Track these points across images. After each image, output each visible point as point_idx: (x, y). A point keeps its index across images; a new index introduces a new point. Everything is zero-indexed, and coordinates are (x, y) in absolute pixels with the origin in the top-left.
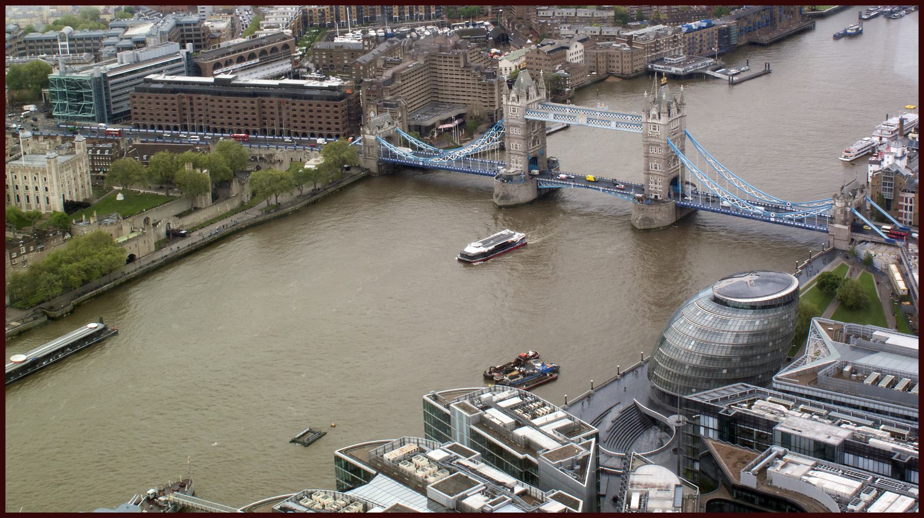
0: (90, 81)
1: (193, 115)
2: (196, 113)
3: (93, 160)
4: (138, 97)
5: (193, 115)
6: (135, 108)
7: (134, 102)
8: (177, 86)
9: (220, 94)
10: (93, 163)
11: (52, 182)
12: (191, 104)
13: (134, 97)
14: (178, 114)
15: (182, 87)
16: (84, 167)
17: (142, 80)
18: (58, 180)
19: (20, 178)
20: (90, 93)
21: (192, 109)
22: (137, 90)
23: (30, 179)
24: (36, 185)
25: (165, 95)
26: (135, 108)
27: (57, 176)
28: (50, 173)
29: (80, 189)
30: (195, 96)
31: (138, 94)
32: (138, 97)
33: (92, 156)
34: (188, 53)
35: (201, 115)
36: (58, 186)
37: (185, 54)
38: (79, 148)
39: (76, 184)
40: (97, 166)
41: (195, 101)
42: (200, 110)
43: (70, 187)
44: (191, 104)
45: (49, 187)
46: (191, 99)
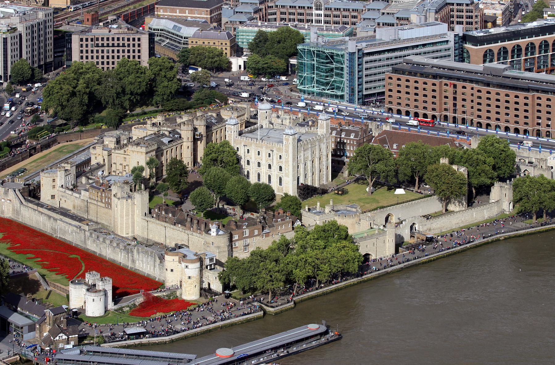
5: (455, 105)
6: (390, 90)
7: (390, 84)
8: (441, 71)
9: (488, 85)
11: (287, 162)
13: (390, 78)
14: (438, 103)
17: (401, 60)
21: (455, 99)
22: (395, 71)
23: (264, 154)
26: (390, 90)
28: (287, 152)
30: (460, 84)
31: (395, 76)
34: (455, 36)
37: (453, 36)
38: (322, 127)
41: (459, 90)
46: (455, 86)
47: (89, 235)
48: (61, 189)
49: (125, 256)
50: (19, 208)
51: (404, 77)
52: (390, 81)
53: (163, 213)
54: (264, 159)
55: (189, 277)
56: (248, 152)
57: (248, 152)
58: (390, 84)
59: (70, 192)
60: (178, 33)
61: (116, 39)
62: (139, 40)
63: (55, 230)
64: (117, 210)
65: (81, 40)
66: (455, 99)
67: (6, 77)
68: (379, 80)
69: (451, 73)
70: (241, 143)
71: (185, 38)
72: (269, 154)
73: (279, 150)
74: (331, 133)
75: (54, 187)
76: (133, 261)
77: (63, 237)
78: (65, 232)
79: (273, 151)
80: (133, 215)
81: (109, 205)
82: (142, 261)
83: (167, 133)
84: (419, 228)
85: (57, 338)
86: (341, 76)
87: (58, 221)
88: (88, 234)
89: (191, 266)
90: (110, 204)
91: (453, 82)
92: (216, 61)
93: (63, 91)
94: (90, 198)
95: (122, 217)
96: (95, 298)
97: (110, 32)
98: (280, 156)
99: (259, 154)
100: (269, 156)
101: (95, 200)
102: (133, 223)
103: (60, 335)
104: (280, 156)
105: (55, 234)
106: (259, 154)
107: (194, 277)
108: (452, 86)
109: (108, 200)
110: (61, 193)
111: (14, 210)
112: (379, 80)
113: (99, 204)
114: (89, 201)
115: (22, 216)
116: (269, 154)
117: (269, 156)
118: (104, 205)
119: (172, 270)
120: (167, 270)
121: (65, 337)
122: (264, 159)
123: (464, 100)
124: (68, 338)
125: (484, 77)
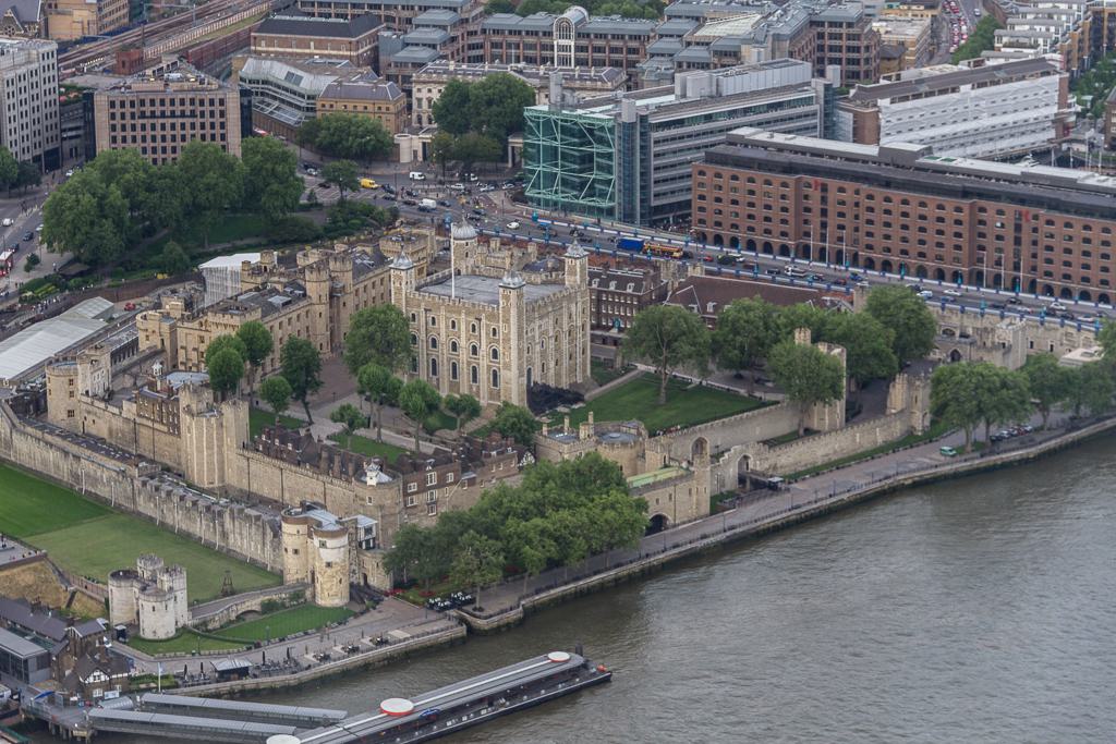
0: (611, 130)
1: (824, 225)
2: (833, 220)
3: (599, 302)
4: (710, 174)
5: (824, 225)
6: (702, 197)
7: (701, 185)
8: (798, 159)
9: (888, 184)
11: (507, 340)
12: (824, 200)
13: (702, 173)
14: (792, 221)
15: (807, 160)
16: (579, 313)
17: (722, 137)
19: (442, 325)
20: (609, 156)
21: (824, 213)
22: (712, 159)
24: (475, 342)
25: (768, 175)
26: (702, 197)
27: (520, 328)
28: (507, 321)
29: (565, 362)
30: (833, 184)
31: (711, 169)
32: (710, 174)
33: (600, 292)
34: (827, 87)
35: (841, 227)
36: (520, 351)
37: (821, 89)
39: (558, 349)
40: (607, 315)
41: (833, 195)
42: (841, 215)
43: (543, 354)
44: (824, 200)
45: (500, 350)
46: (824, 188)
48: (85, 399)
49: (208, 526)
51: (727, 171)
52: (701, 178)
53: (277, 442)
54: (463, 335)
55: (329, 565)
56: (434, 323)
57: (434, 323)
58: (701, 185)
59: (102, 405)
60: (295, 88)
61: (177, 102)
62: (222, 102)
63: (77, 477)
65: (112, 104)
66: (824, 213)
68: (682, 177)
69: (817, 161)
71: (309, 98)
72: (474, 326)
73: (493, 317)
74: (590, 284)
75: (72, 394)
76: (224, 535)
78: (95, 481)
80: (220, 447)
81: (175, 429)
82: (241, 534)
83: (279, 287)
84: (755, 465)
85: (91, 680)
86: (609, 170)
87: (82, 460)
88: (138, 483)
89: (330, 543)
91: (820, 179)
92: (370, 140)
93: (80, 207)
95: (200, 451)
96: (157, 605)
98: (494, 329)
99: (454, 327)
100: (474, 330)
101: (148, 419)
102: (221, 463)
103: (95, 674)
104: (494, 329)
105: (78, 484)
106: (454, 327)
108: (819, 188)
110: (84, 407)
112: (682, 177)
113: (157, 426)
114: (138, 420)
115: (16, 452)
116: (474, 326)
117: (474, 330)
118: (165, 429)
119: (296, 552)
120: (286, 550)
121: (103, 678)
122: (463, 335)
123: (841, 215)
124: (111, 679)
125: (879, 170)
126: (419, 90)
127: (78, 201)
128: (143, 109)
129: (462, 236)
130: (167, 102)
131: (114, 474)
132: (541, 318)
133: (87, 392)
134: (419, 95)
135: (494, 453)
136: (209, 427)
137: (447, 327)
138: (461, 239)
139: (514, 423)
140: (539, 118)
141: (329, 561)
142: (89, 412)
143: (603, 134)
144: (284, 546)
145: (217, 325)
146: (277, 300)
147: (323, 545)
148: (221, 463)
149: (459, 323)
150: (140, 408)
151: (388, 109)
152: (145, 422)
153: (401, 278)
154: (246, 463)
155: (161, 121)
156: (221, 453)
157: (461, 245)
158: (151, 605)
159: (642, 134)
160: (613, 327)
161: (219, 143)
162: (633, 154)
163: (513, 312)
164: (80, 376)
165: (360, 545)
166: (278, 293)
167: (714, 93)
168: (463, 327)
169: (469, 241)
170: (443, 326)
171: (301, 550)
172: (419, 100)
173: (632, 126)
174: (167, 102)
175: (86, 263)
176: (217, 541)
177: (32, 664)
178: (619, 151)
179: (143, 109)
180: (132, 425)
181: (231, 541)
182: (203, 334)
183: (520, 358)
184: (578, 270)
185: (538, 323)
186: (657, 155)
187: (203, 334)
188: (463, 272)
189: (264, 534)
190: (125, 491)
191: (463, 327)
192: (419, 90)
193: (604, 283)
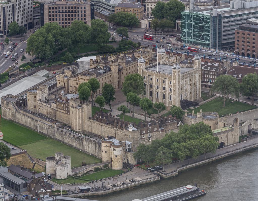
0: (209, 19)
3: (204, 74)
4: (241, 33)
6: (238, 41)
7: (238, 37)
10: (204, 76)
11: (175, 85)
13: (238, 33)
16: (198, 77)
17: (245, 21)
18: (179, 84)
19: (154, 80)
20: (209, 27)
22: (241, 28)
24: (164, 86)
26: (238, 41)
27: (179, 82)
28: (175, 79)
29: (193, 92)
31: (241, 31)
32: (241, 33)
33: (205, 71)
36: (179, 89)
38: (196, 64)
39: (191, 89)
40: (207, 78)
43: (186, 90)
45: (172, 89)
47: (56, 130)
48: (39, 102)
50: (15, 113)
51: (246, 32)
52: (238, 35)
54: (161, 84)
55: (116, 156)
56: (151, 80)
57: (151, 80)
58: (238, 37)
59: (45, 104)
60: (108, 4)
61: (70, 8)
62: (85, 8)
64: (73, 115)
65: (50, 8)
67: (5, 32)
68: (232, 34)
70: (147, 74)
71: (112, 7)
72: (164, 81)
73: (170, 78)
74: (202, 68)
76: (83, 146)
77: (41, 131)
78: (42, 128)
79: (166, 79)
80: (82, 118)
81: (68, 112)
82: (88, 146)
83: (102, 67)
84: (253, 127)
85: (40, 191)
86: (208, 31)
87: (38, 122)
88: (56, 129)
89: (117, 149)
90: (69, 112)
92: (132, 21)
93: (39, 41)
94: (57, 108)
97: (67, 2)
98: (170, 82)
100: (164, 82)
101: (59, 109)
102: (83, 123)
103: (41, 190)
104: (170, 82)
105: (37, 129)
107: (119, 156)
109: (67, 109)
110: (39, 105)
111: (12, 114)
112: (232, 34)
113: (62, 111)
114: (56, 109)
116: (164, 81)
117: (164, 82)
118: (65, 112)
119: (106, 152)
120: (103, 151)
122: (161, 84)
126: (148, 5)
127: (38, 39)
128: (59, 10)
129: (161, 52)
130: (67, 8)
131: (48, 126)
132: (186, 78)
133: (40, 100)
134: (148, 7)
135: (170, 121)
136: (79, 111)
137: (155, 81)
138: (160, 53)
139: (176, 112)
140: (186, 14)
141: (116, 155)
142: (40, 106)
143: (207, 20)
144: (102, 150)
145: (82, 79)
146: (101, 71)
147: (115, 150)
148: (83, 123)
149: (159, 80)
150: (57, 105)
151: (138, 11)
152: (58, 110)
153: (141, 65)
154: (90, 123)
155: (65, 14)
156: (82, 120)
157: (160, 55)
158: (59, 168)
159: (219, 20)
160: (209, 82)
161: (83, 21)
162: (216, 27)
163: (177, 77)
164: (38, 95)
165: (127, 151)
166: (101, 69)
167: (243, 7)
168: (161, 81)
169: (163, 54)
170: (154, 81)
171: (108, 153)
172: (148, 8)
173: (216, 17)
174: (67, 8)
175: (40, 59)
176: (81, 148)
177: (21, 186)
178: (212, 25)
179: (59, 10)
180: (54, 111)
181: (85, 148)
182: (77, 82)
183: (179, 91)
184: (198, 63)
185: (185, 80)
186: (224, 27)
187: (77, 82)
188: (161, 63)
189: (96, 146)
190: (52, 131)
191: (161, 81)
192: (148, 5)
193: (206, 68)
